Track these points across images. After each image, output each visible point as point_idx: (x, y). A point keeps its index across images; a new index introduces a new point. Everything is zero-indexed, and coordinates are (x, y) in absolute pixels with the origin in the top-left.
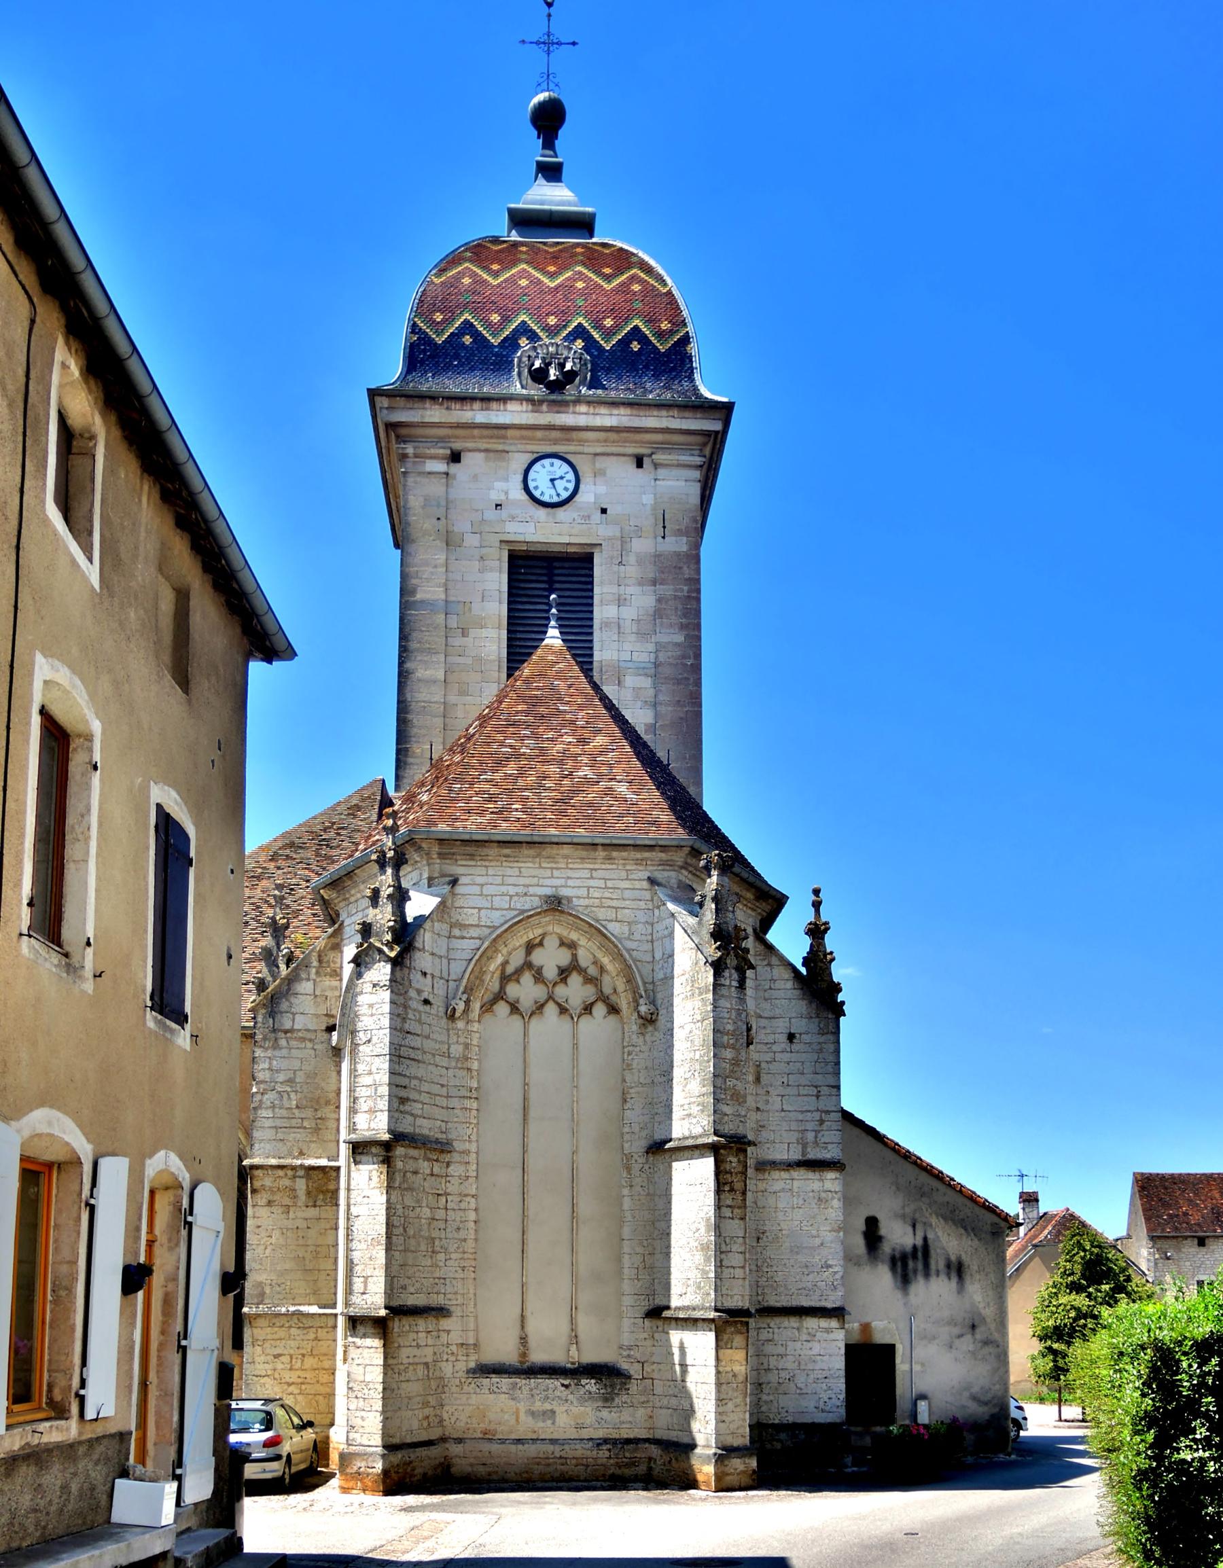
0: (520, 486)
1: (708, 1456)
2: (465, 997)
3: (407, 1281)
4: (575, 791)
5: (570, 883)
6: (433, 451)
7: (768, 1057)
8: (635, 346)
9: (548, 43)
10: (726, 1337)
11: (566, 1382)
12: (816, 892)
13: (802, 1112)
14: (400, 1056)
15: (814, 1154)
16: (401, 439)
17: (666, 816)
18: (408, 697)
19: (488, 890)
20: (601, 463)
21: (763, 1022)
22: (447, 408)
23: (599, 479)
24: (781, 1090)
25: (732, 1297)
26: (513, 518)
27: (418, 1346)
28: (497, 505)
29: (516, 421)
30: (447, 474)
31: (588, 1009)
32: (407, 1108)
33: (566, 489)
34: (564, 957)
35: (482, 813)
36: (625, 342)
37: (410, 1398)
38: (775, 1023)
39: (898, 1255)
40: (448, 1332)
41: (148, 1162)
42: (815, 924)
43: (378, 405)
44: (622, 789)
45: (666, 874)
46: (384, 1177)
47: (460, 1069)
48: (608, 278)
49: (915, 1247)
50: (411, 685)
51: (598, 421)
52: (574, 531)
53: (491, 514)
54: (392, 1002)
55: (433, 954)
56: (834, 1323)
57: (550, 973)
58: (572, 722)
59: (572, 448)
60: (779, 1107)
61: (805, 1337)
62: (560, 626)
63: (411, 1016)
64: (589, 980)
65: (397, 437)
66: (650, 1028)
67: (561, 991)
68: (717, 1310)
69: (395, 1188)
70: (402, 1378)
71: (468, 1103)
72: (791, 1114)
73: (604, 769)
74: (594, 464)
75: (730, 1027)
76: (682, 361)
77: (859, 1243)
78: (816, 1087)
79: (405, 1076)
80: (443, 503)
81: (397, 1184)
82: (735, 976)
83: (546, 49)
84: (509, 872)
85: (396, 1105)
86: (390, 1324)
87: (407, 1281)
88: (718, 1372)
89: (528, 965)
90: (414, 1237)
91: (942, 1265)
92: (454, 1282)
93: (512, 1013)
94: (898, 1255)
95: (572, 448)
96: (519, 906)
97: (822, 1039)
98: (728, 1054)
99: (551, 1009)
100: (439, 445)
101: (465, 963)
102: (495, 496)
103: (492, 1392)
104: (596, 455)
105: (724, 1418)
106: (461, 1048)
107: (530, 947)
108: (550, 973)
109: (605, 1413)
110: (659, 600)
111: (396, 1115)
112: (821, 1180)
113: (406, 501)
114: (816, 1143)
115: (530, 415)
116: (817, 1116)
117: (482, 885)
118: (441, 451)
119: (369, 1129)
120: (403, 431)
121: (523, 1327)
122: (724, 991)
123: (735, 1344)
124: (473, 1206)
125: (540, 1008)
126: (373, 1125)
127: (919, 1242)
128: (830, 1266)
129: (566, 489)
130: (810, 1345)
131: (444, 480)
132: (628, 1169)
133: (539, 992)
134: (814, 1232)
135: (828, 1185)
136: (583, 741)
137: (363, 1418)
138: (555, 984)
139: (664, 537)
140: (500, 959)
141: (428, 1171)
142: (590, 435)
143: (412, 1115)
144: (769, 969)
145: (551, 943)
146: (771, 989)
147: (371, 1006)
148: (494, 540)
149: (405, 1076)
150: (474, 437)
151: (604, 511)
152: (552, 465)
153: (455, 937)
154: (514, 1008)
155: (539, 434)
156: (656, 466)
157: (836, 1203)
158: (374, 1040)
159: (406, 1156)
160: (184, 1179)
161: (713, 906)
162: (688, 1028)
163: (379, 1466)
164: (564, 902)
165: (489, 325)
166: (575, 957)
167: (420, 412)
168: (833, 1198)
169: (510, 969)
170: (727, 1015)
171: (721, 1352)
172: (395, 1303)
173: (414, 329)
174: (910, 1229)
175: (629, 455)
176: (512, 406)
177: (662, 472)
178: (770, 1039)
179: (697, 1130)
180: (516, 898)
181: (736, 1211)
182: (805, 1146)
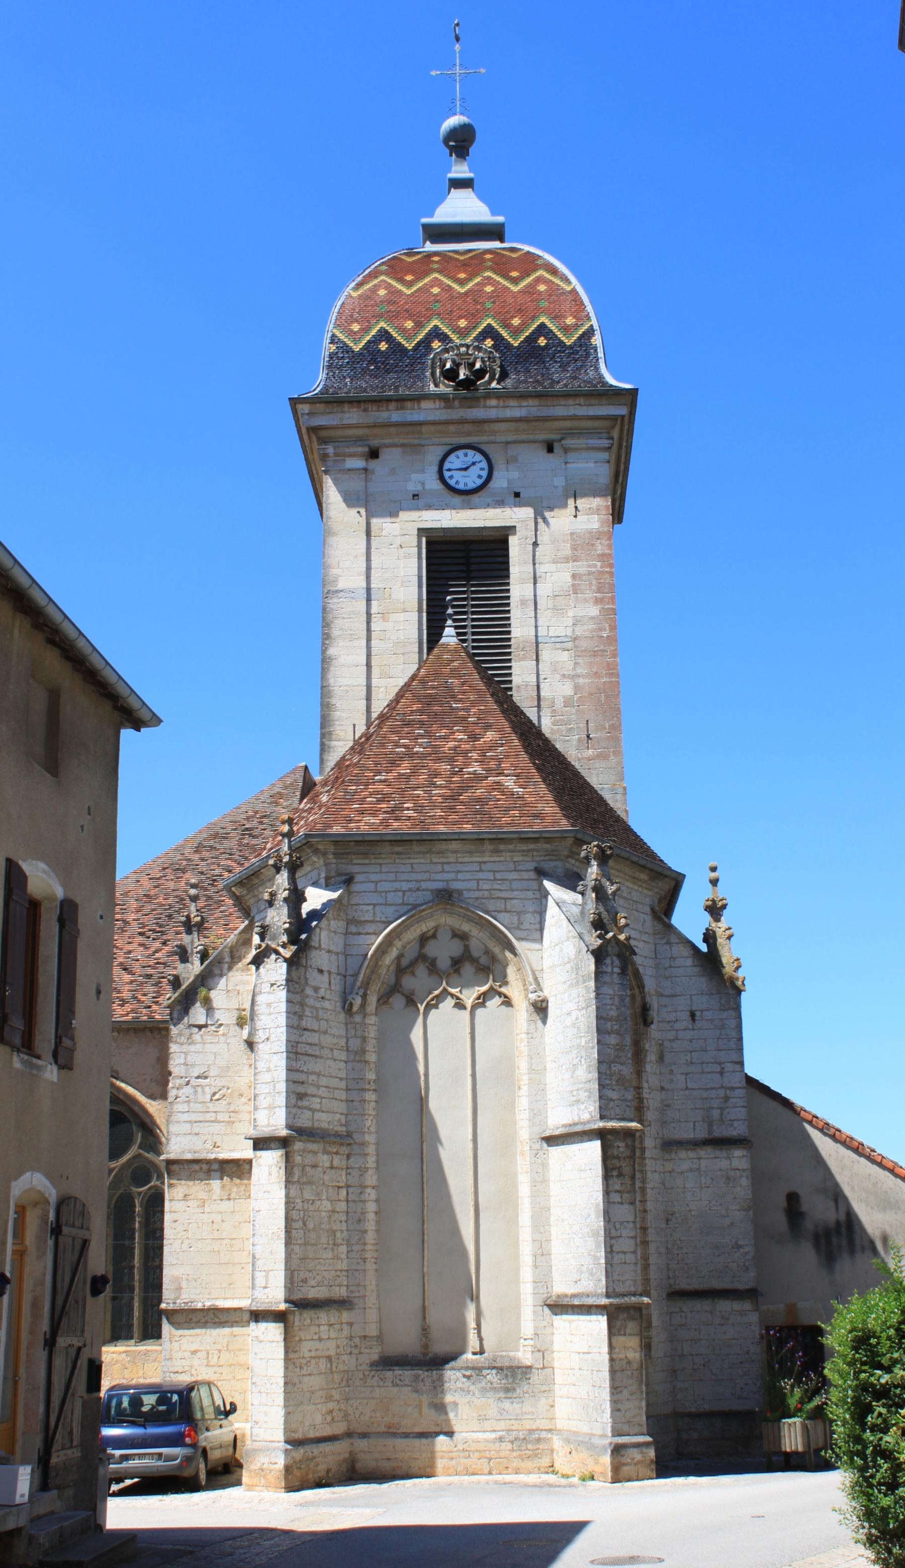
1: (604, 1447)
2: (361, 992)
3: (307, 1275)
4: (464, 788)
5: (460, 876)
10: (618, 1323)
13: (707, 1089)
14: (297, 1053)
15: (717, 1133)
16: (323, 441)
17: (549, 808)
20: (513, 450)
21: (665, 1001)
22: (365, 410)
25: (623, 1282)
27: (320, 1339)
32: (305, 1103)
34: (455, 948)
35: (374, 814)
37: (312, 1392)
41: (14, 1184)
42: (713, 901)
44: (509, 783)
45: (552, 864)
46: (283, 1172)
47: (358, 1061)
51: (508, 413)
54: (289, 1001)
55: (329, 951)
57: (444, 963)
58: (465, 718)
59: (485, 438)
60: (684, 1086)
63: (307, 1013)
68: (608, 1296)
69: (293, 1183)
70: (304, 1372)
73: (493, 764)
75: (613, 1013)
78: (720, 1064)
79: (302, 1072)
81: (296, 1179)
82: (617, 962)
84: (403, 868)
85: (293, 1101)
86: (291, 1318)
87: (307, 1275)
88: (612, 1360)
90: (314, 1229)
92: (357, 1274)
95: (485, 438)
96: (411, 901)
97: (724, 1015)
98: (613, 1040)
100: (358, 443)
103: (395, 1385)
104: (507, 443)
105: (619, 1406)
106: (358, 1042)
108: (444, 963)
109: (507, 1404)
111: (294, 1110)
112: (729, 1158)
114: (721, 1120)
115: (444, 411)
116: (721, 1093)
117: (376, 883)
119: (268, 1125)
120: (324, 434)
121: (424, 1318)
122: (607, 978)
123: (628, 1331)
126: (272, 1122)
135: (736, 1163)
136: (474, 737)
137: (266, 1414)
141: (328, 1164)
142: (502, 426)
143: (310, 1109)
144: (668, 947)
145: (444, 936)
146: (671, 967)
147: (269, 1005)
149: (302, 1072)
152: (466, 455)
153: (351, 933)
155: (452, 428)
156: (566, 450)
157: (744, 1182)
158: (272, 1038)
159: (304, 1151)
160: (50, 1195)
161: (594, 895)
162: (574, 1014)
163: (280, 1461)
164: (455, 895)
167: (340, 415)
168: (741, 1177)
169: (405, 962)
170: (609, 1002)
171: (614, 1339)
172: (296, 1297)
175: (540, 442)
176: (425, 404)
178: (672, 1017)
179: (586, 1116)
180: (408, 894)
181: (625, 1195)
182: (710, 1125)
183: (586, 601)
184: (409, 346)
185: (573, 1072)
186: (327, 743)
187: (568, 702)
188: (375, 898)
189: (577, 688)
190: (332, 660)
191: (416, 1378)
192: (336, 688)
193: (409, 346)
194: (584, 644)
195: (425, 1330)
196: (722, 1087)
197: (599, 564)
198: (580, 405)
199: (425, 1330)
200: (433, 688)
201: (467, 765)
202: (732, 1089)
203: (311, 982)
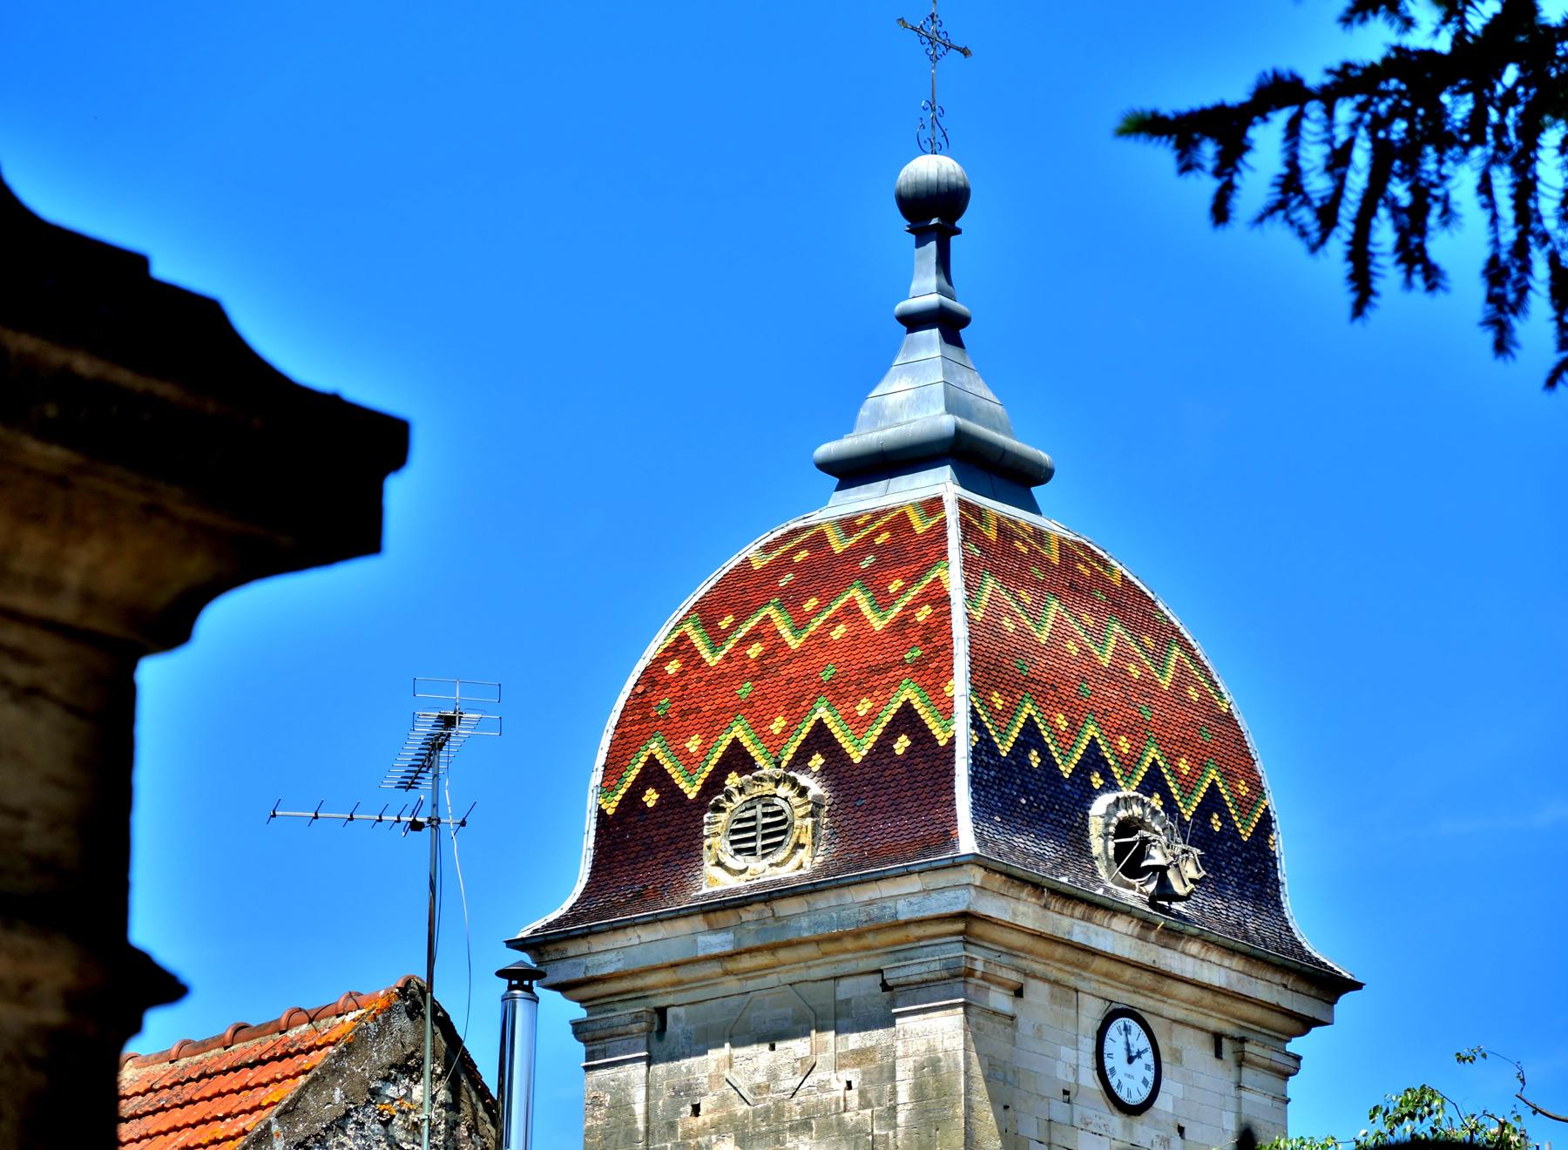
74: (1170, 1039)
155: (1129, 973)
167: (1013, 904)
176: (1120, 923)
198: (1285, 986)
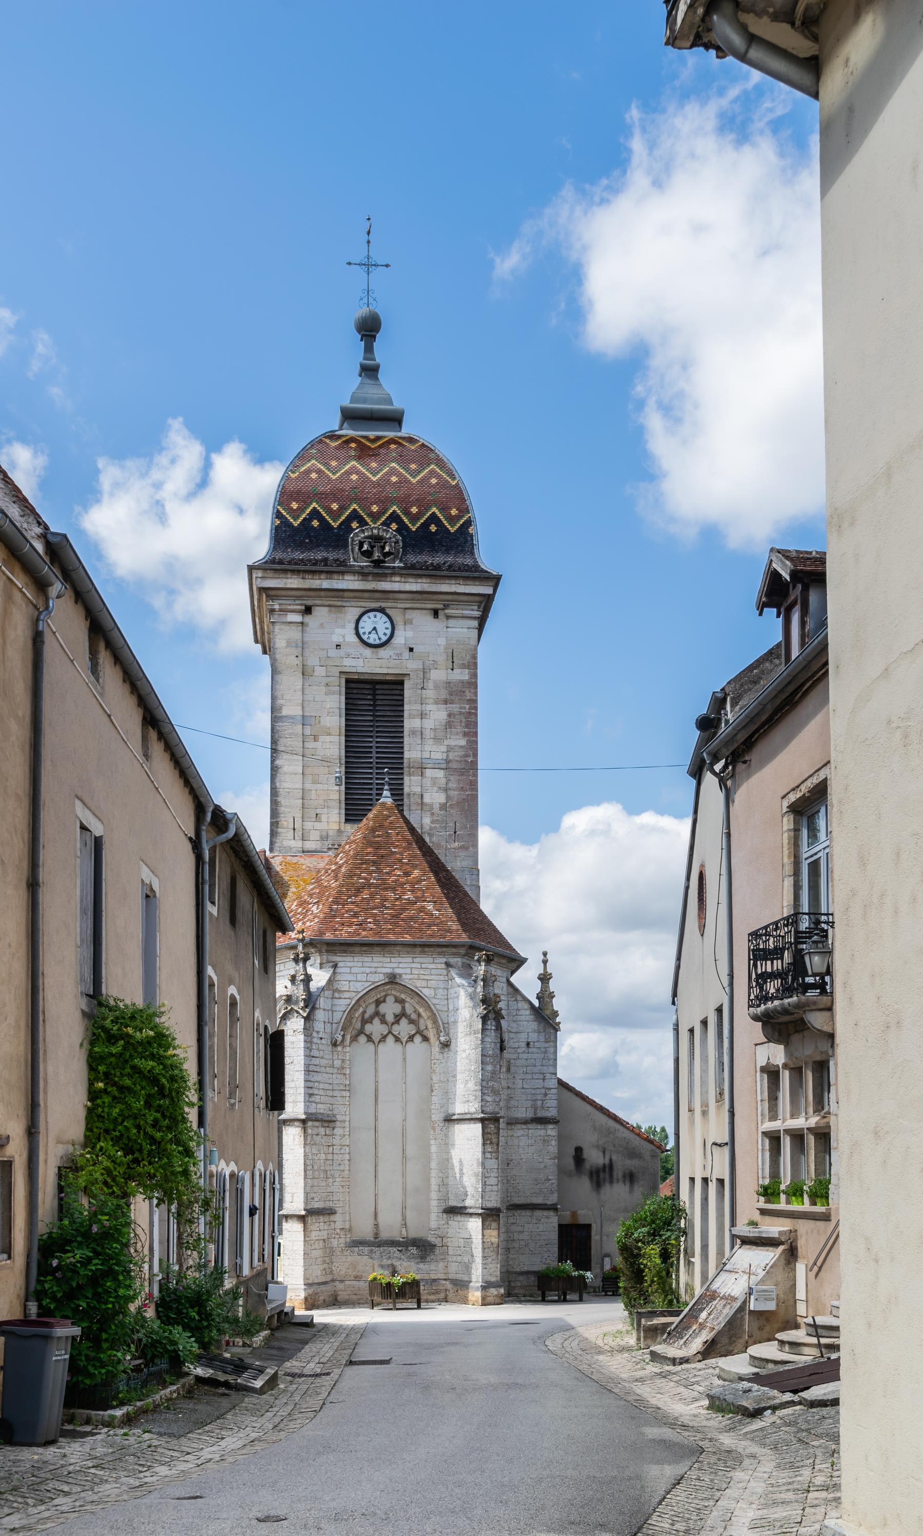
0: (353, 632)
1: (478, 1287)
2: (342, 1033)
3: (314, 1195)
4: (404, 910)
5: (401, 965)
6: (292, 607)
7: (514, 1056)
8: (433, 528)
9: (368, 265)
10: (487, 1223)
11: (400, 1249)
12: (545, 954)
14: (309, 1071)
15: (540, 1114)
17: (455, 926)
18: (278, 784)
19: (354, 970)
21: (512, 1035)
22: (303, 578)
23: (408, 627)
24: (522, 1076)
25: (491, 1201)
26: (348, 656)
27: (320, 1230)
28: (337, 646)
29: (351, 587)
30: (302, 623)
31: (411, 1038)
32: (313, 1099)
33: (385, 634)
34: (397, 1009)
35: (350, 925)
36: (426, 525)
37: (317, 1259)
38: (519, 1035)
39: (594, 1170)
40: (335, 1222)
42: (544, 975)
43: (254, 576)
44: (430, 907)
45: (456, 960)
46: (302, 1138)
48: (414, 474)
49: (604, 1165)
50: (279, 777)
52: (391, 665)
53: (333, 653)
54: (305, 1041)
55: (324, 1010)
56: (552, 1213)
57: (390, 1018)
59: (389, 604)
61: (534, 1221)
62: (391, 790)
63: (314, 1047)
64: (411, 1022)
65: (268, 596)
66: (446, 1049)
67: (396, 1029)
68: (482, 1209)
69: (307, 1144)
70: (313, 1248)
71: (344, 1093)
72: (527, 1090)
73: (419, 894)
74: (404, 615)
75: (490, 1052)
76: (466, 541)
77: (570, 1163)
78: (543, 1074)
80: (300, 644)
81: (308, 1142)
82: (494, 1023)
83: (366, 269)
84: (366, 959)
85: (307, 1098)
86: (307, 1219)
87: (314, 1195)
88: (483, 1242)
89: (377, 1014)
90: (317, 1170)
91: (620, 1175)
92: (338, 1194)
93: (368, 1041)
94: (594, 1170)
96: (372, 979)
97: (547, 1045)
98: (489, 1068)
99: (390, 1039)
101: (342, 1013)
102: (336, 639)
104: (406, 609)
105: (486, 1266)
106: (340, 1062)
107: (378, 1003)
108: (390, 1018)
109: (421, 1266)
110: (449, 715)
111: (307, 1104)
113: (275, 644)
114: (542, 1107)
115: (361, 582)
116: (543, 1091)
117: (351, 967)
118: (299, 607)
119: (293, 1112)
121: (376, 1218)
122: (488, 1033)
123: (492, 1227)
124: (347, 1151)
125: (383, 1038)
126: (295, 1110)
127: (607, 1161)
128: (550, 1180)
129: (385, 634)
130: (537, 1225)
131: (300, 628)
132: (434, 1129)
133: (384, 1029)
134: (541, 1160)
135: (549, 1132)
136: (407, 874)
137: (292, 1270)
138: (393, 1024)
139: (452, 669)
140: (361, 1010)
141: (323, 1133)
143: (315, 1103)
145: (390, 999)
147: (293, 1043)
148: (336, 672)
150: (321, 597)
151: (411, 650)
153: (336, 998)
154: (370, 1039)
155: (366, 595)
156: (448, 617)
157: (553, 1143)
158: (295, 1062)
161: (482, 983)
162: (468, 1052)
163: (302, 1295)
164: (398, 977)
165: (329, 511)
166: (403, 1008)
167: (284, 580)
168: (552, 1140)
169: (367, 1016)
170: (489, 1046)
171: (485, 1232)
172: (308, 1207)
173: (278, 515)
174: (601, 1154)
177: (452, 622)
178: (516, 1045)
179: (473, 1110)
180: (370, 975)
181: (494, 1154)
182: (536, 1109)
183: (457, 734)
184: (335, 525)
185: (466, 1084)
186: (275, 829)
187: (443, 807)
188: (350, 977)
189: (448, 798)
190: (278, 768)
191: (371, 1251)
192: (281, 790)
193: (335, 525)
194: (454, 765)
195: (376, 1226)
196: (544, 1088)
197: (467, 706)
199: (376, 1226)
200: (379, 836)
201: (404, 894)
202: (550, 1089)
203: (316, 1029)
